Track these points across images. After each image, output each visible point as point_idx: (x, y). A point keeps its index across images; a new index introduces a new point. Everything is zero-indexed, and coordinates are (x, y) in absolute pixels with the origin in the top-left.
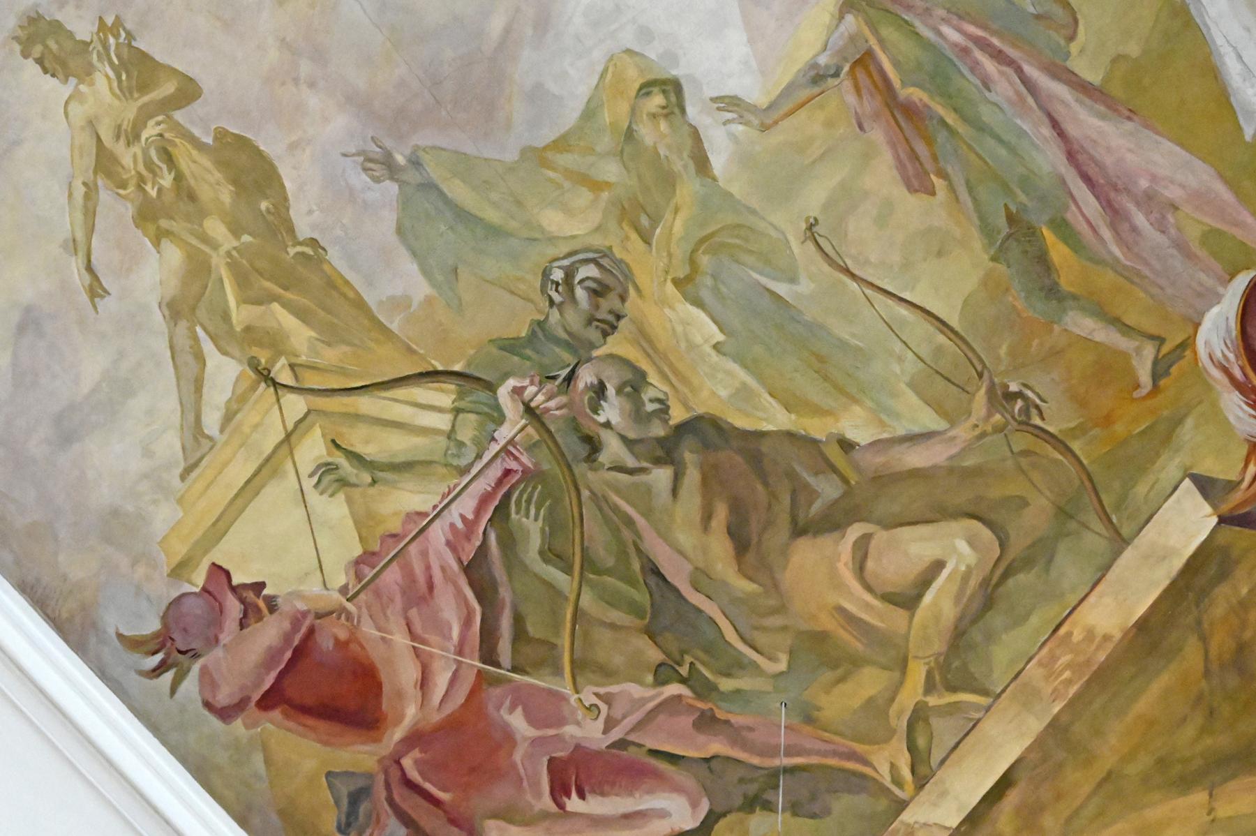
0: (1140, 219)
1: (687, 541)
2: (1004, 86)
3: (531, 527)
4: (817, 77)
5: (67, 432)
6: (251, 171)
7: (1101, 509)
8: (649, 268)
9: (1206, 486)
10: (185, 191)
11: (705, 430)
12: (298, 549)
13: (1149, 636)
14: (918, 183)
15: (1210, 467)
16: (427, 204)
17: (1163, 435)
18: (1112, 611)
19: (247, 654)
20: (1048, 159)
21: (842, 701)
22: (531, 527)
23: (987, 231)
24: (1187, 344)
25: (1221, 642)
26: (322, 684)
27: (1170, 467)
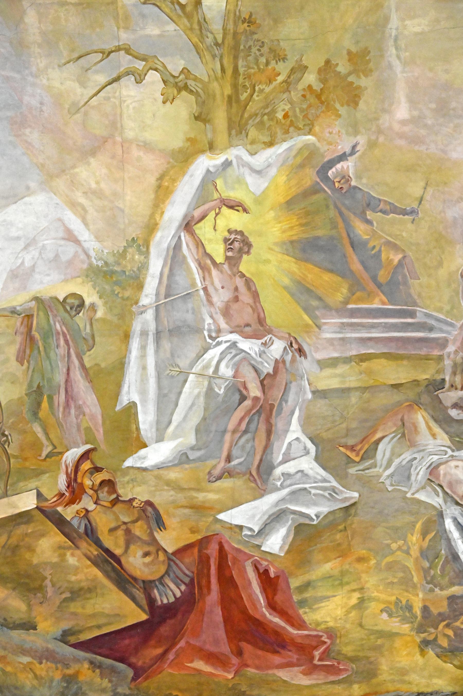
0: (73, 411)
2: (62, 350)
4: (14, 312)
9: (39, 495)
14: (20, 359)
15: (44, 491)
17: (38, 473)
20: (60, 378)
23: (30, 385)
24: (62, 453)
25: (13, 541)
27: (33, 484)
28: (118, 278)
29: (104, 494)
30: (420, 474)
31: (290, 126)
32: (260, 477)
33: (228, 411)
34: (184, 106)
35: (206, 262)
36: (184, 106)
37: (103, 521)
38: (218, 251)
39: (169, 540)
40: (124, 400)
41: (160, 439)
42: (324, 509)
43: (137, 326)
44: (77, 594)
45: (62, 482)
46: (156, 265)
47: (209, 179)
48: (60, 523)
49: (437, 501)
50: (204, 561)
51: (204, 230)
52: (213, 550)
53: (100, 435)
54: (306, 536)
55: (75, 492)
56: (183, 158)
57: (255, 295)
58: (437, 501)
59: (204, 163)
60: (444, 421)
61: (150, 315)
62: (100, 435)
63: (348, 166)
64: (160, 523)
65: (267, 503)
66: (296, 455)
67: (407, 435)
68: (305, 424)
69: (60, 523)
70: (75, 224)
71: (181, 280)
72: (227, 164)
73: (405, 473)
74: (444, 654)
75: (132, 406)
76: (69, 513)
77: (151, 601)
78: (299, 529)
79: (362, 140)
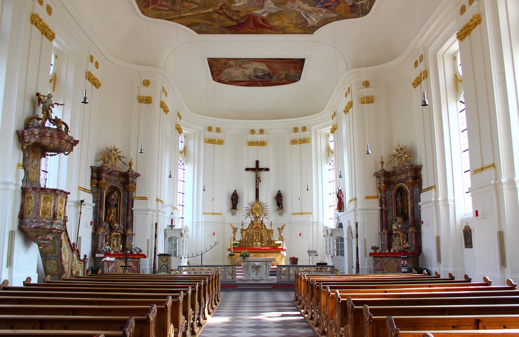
7: (206, 7)
13: (204, 13)
17: (213, 7)
18: (202, 12)
21: (182, 9)
29: (228, 9)
30: (296, 7)
32: (262, 7)
37: (228, 13)
41: (240, 2)
42: (275, 11)
44: (222, 21)
45: (218, 8)
52: (251, 16)
54: (271, 15)
55: (221, 8)
64: (240, 13)
65: (263, 10)
73: (293, 7)
74: (300, 28)
76: (220, 12)
77: (238, 23)
78: (270, 13)
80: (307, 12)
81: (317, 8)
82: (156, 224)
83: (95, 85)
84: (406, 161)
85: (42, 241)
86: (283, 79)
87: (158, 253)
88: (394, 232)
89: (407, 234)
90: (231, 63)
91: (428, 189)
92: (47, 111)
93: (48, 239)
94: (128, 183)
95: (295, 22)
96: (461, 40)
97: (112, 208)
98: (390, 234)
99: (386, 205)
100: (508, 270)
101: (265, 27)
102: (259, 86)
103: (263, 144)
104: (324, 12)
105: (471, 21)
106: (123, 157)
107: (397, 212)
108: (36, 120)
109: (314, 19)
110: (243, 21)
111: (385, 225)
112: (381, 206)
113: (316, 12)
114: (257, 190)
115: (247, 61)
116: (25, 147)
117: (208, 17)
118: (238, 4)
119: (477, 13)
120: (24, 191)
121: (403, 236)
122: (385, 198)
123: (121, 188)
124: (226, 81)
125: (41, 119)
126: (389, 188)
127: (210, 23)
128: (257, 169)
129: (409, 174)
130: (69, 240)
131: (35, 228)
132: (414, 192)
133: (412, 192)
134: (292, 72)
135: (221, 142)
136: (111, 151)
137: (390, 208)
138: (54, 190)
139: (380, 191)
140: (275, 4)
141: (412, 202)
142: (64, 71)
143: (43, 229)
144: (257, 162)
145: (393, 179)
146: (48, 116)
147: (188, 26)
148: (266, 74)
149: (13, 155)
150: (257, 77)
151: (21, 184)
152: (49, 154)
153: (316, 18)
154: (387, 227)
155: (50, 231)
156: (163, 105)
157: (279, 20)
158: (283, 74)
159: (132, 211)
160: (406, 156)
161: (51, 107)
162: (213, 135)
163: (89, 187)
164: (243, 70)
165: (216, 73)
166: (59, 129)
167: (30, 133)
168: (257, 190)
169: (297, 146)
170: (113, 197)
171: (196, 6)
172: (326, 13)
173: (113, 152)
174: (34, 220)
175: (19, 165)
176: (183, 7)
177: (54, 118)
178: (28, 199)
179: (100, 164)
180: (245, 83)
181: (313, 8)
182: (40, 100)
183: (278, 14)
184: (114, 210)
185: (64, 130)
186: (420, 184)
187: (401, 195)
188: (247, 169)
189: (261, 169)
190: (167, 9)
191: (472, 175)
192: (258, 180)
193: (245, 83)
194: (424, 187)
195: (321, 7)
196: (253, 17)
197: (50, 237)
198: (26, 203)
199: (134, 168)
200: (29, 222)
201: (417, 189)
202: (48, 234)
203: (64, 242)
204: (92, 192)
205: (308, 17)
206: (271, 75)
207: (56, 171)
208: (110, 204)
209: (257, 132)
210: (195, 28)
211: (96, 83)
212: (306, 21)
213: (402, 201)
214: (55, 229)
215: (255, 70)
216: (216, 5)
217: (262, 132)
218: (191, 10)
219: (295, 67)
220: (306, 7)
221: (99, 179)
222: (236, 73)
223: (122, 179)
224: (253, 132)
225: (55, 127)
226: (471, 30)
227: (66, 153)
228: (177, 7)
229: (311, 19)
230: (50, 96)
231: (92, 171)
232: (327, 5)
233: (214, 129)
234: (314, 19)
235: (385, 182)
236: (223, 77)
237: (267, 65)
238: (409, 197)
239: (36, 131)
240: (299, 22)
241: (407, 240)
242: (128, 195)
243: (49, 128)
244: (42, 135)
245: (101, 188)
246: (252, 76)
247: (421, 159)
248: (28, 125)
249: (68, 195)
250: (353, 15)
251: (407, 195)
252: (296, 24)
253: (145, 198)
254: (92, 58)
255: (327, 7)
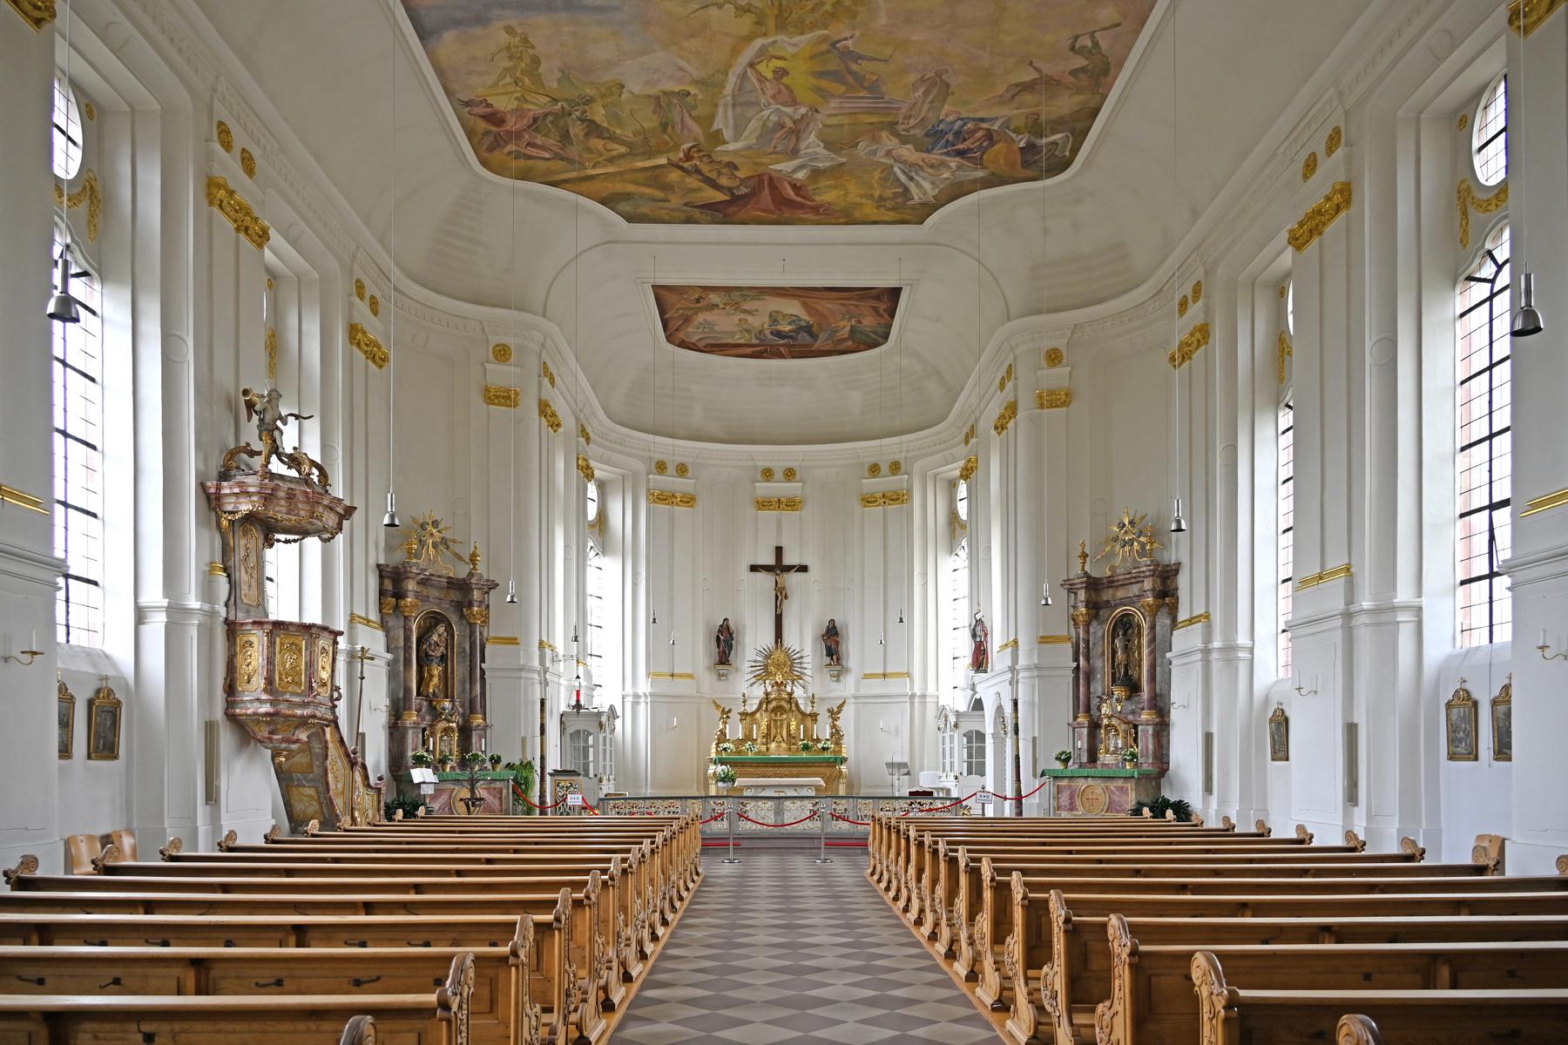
1: (577, 130)
3: (550, 118)
5: (470, 73)
6: (536, 61)
7: (650, 154)
8: (600, 101)
10: (521, 58)
11: (592, 122)
12: (502, 103)
13: (645, 169)
16: (565, 77)
18: (640, 164)
19: (481, 110)
20: (678, 119)
22: (550, 118)
26: (495, 118)
28: (711, 85)
31: (814, 26)
32: (794, 153)
33: (774, 131)
34: (748, 20)
35: (762, 79)
36: (748, 20)
37: (705, 168)
38: (770, 75)
39: (741, 174)
40: (715, 127)
41: (736, 140)
43: (721, 102)
45: (681, 155)
46: (732, 81)
47: (763, 49)
48: (682, 169)
49: (891, 162)
50: (761, 182)
51: (762, 67)
52: (766, 178)
53: (702, 139)
54: (816, 174)
55: (688, 157)
56: (748, 39)
57: (791, 91)
58: (891, 162)
59: (758, 42)
60: (896, 134)
61: (729, 99)
62: (702, 139)
63: (849, 43)
64: (736, 168)
65: (796, 162)
66: (812, 144)
67: (875, 139)
68: (818, 136)
69: (682, 169)
70: (683, 63)
71: (747, 86)
72: (775, 42)
73: (874, 153)
75: (719, 131)
76: (686, 165)
77: (732, 194)
79: (857, 33)
80: (910, 168)
81: (934, 157)
82: (543, 702)
83: (373, 359)
84: (1142, 552)
85: (284, 745)
86: (845, 340)
87: (549, 769)
88: (1105, 721)
89: (1136, 727)
90: (714, 298)
91: (1191, 621)
92: (270, 431)
93: (297, 741)
94: (470, 605)
95: (877, 194)
96: (1298, 248)
97: (434, 665)
98: (1094, 726)
99: (1088, 659)
100: (1360, 813)
101: (801, 206)
102: (782, 356)
103: (792, 504)
104: (953, 165)
105: (1328, 199)
106: (454, 541)
107: (1114, 674)
108: (245, 456)
109: (927, 185)
110: (744, 191)
111: (1084, 705)
112: (1076, 659)
113: (932, 166)
114: (779, 620)
115: (753, 293)
116: (225, 523)
117: (654, 177)
118: (731, 147)
119: (1342, 179)
120: (232, 628)
121: (1126, 732)
122: (1087, 642)
123: (454, 619)
124: (701, 345)
125: (259, 453)
126: (1096, 616)
127: (660, 194)
128: (779, 567)
129: (1148, 584)
130: (342, 741)
131: (267, 714)
132: (1158, 628)
133: (1153, 628)
134: (869, 322)
135: (689, 500)
136: (423, 526)
137: (1098, 664)
138: (307, 628)
139: (1076, 625)
140: (828, 145)
141: (1153, 652)
142: (293, 321)
143: (287, 716)
144: (779, 551)
145: (1107, 595)
146: (275, 449)
147: (603, 202)
148: (801, 328)
149: (195, 543)
150: (778, 334)
151: (223, 611)
152: (282, 537)
153: (933, 183)
154: (1088, 709)
155: (303, 722)
156: (544, 408)
157: (835, 187)
158: (845, 327)
159: (483, 672)
160: (1142, 539)
161: (279, 423)
162: (670, 482)
163: (374, 616)
164: (743, 316)
165: (673, 325)
166: (306, 480)
167: (237, 490)
168: (779, 620)
169: (878, 510)
170: (435, 638)
171: (623, 149)
172: (960, 167)
173: (430, 528)
174: (264, 697)
175: (212, 569)
176: (590, 150)
177: (289, 450)
178: (244, 647)
179: (398, 557)
180: (749, 350)
181: (925, 155)
182: (250, 406)
183: (836, 171)
184: (437, 670)
185: (316, 479)
186: (1173, 610)
187: (1125, 634)
188: (754, 568)
189: (789, 568)
190: (547, 155)
191: (1295, 590)
192: (780, 595)
193: (749, 350)
194: (1183, 615)
195: (947, 154)
196: (771, 178)
197: (303, 736)
198: (240, 657)
199: (481, 568)
200: (251, 701)
201: (1163, 621)
202: (297, 727)
203: (330, 745)
204: (383, 625)
205: (911, 179)
206: (815, 329)
207: (295, 580)
208: (427, 655)
209: (779, 475)
210: (625, 207)
211: (376, 356)
212: (906, 190)
213: (1126, 649)
214: (314, 716)
215: (774, 318)
216: (676, 147)
217: (790, 474)
218: (611, 160)
219: (875, 309)
220: (908, 152)
221: (399, 595)
222: (725, 324)
223: (455, 595)
224: (768, 474)
225: (293, 473)
226: (1324, 224)
227: (326, 536)
228: (573, 151)
229: (918, 185)
230: (275, 396)
231: (381, 577)
232: (961, 146)
233: (671, 469)
234: (927, 185)
235: (1088, 604)
236: (693, 333)
237: (805, 305)
238: (1145, 640)
239: (252, 482)
240: (889, 193)
241: (1136, 740)
242: (472, 633)
243: (282, 477)
244: (268, 498)
245: (406, 618)
246: (767, 332)
247: (1177, 551)
248: (228, 469)
249: (340, 639)
250: (1030, 173)
251: (1140, 635)
252: (881, 198)
253: (513, 641)
254: (360, 288)
255: (960, 153)
